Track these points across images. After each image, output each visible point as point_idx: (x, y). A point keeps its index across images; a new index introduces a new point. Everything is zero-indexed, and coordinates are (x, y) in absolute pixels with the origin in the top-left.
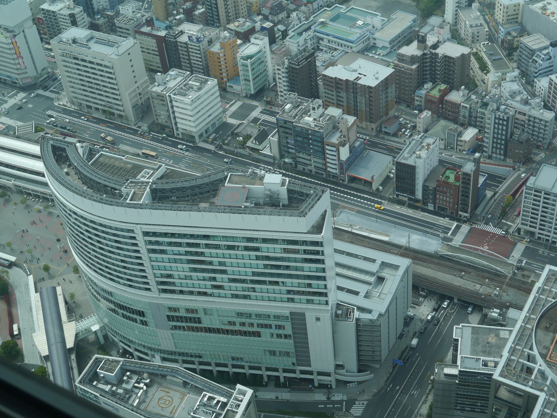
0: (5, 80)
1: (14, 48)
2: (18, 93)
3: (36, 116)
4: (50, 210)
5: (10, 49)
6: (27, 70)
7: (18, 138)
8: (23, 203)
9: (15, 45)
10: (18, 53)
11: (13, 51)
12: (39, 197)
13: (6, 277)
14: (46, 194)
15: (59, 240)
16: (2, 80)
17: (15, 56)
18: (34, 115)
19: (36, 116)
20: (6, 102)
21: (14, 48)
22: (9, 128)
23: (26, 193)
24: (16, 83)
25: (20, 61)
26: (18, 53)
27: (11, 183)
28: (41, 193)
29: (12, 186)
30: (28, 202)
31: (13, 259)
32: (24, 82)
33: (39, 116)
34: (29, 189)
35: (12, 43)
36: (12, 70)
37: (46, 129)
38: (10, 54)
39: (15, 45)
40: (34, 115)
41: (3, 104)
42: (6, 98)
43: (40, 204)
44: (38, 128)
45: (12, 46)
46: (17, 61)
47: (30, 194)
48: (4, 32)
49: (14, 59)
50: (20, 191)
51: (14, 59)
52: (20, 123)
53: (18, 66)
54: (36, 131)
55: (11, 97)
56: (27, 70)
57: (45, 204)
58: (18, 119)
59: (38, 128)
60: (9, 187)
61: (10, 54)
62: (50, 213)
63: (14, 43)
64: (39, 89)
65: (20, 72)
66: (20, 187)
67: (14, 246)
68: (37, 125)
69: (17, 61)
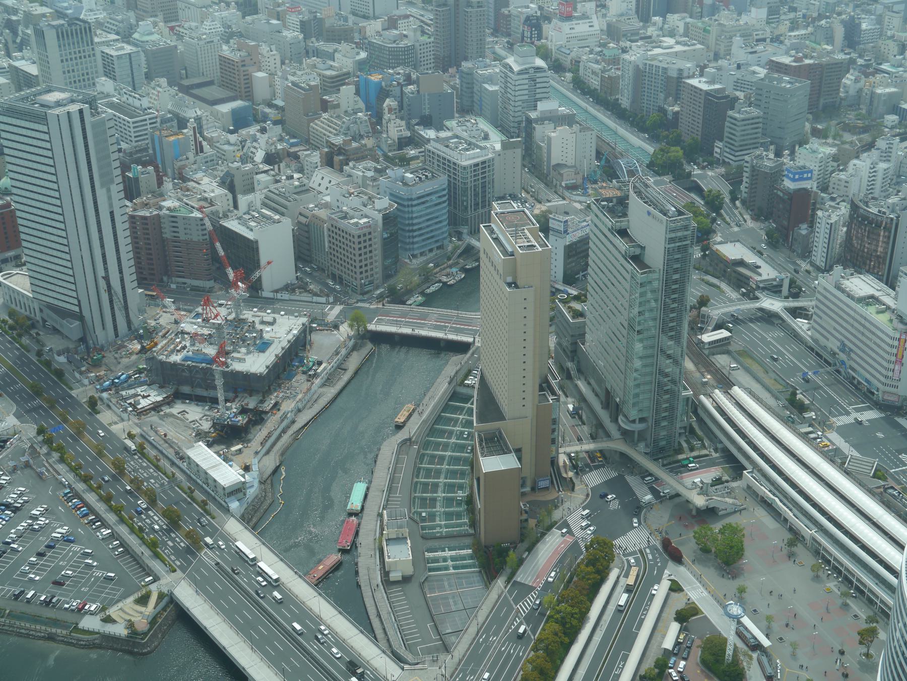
0: (859, 383)
1: (898, 348)
2: (870, 408)
3: (883, 453)
4: (848, 601)
5: (892, 346)
6: (899, 384)
7: (847, 473)
8: (813, 571)
9: (902, 344)
10: (899, 356)
11: (895, 351)
12: (839, 573)
13: (745, 664)
14: (853, 576)
15: (842, 653)
16: (856, 382)
17: (893, 359)
18: (881, 451)
19: (883, 453)
20: (848, 413)
21: (898, 348)
22: (837, 451)
23: (823, 557)
24: (873, 394)
25: (897, 367)
26: (899, 356)
27: (809, 532)
28: (847, 570)
29: (808, 537)
30: (820, 573)
31: (766, 643)
32: (886, 397)
33: (889, 458)
34: (831, 555)
35: (899, 340)
36: (878, 375)
37: (889, 479)
38: (888, 353)
39: (902, 344)
40: (881, 451)
41: (843, 415)
42: (850, 408)
43: (836, 583)
44: (878, 473)
45: (896, 343)
46: (892, 366)
47: (828, 562)
48: (895, 321)
49: (889, 362)
50: (817, 551)
51: (889, 362)
52: (856, 454)
53: (890, 374)
54: (874, 476)
55: (857, 410)
56: (899, 384)
57: (844, 589)
58: (856, 446)
59: (878, 473)
60: (803, 537)
61: (888, 353)
62: (846, 605)
63: (902, 341)
64: (903, 416)
65: (888, 382)
66: (820, 545)
67: (775, 626)
68: (879, 468)
69: (892, 366)
